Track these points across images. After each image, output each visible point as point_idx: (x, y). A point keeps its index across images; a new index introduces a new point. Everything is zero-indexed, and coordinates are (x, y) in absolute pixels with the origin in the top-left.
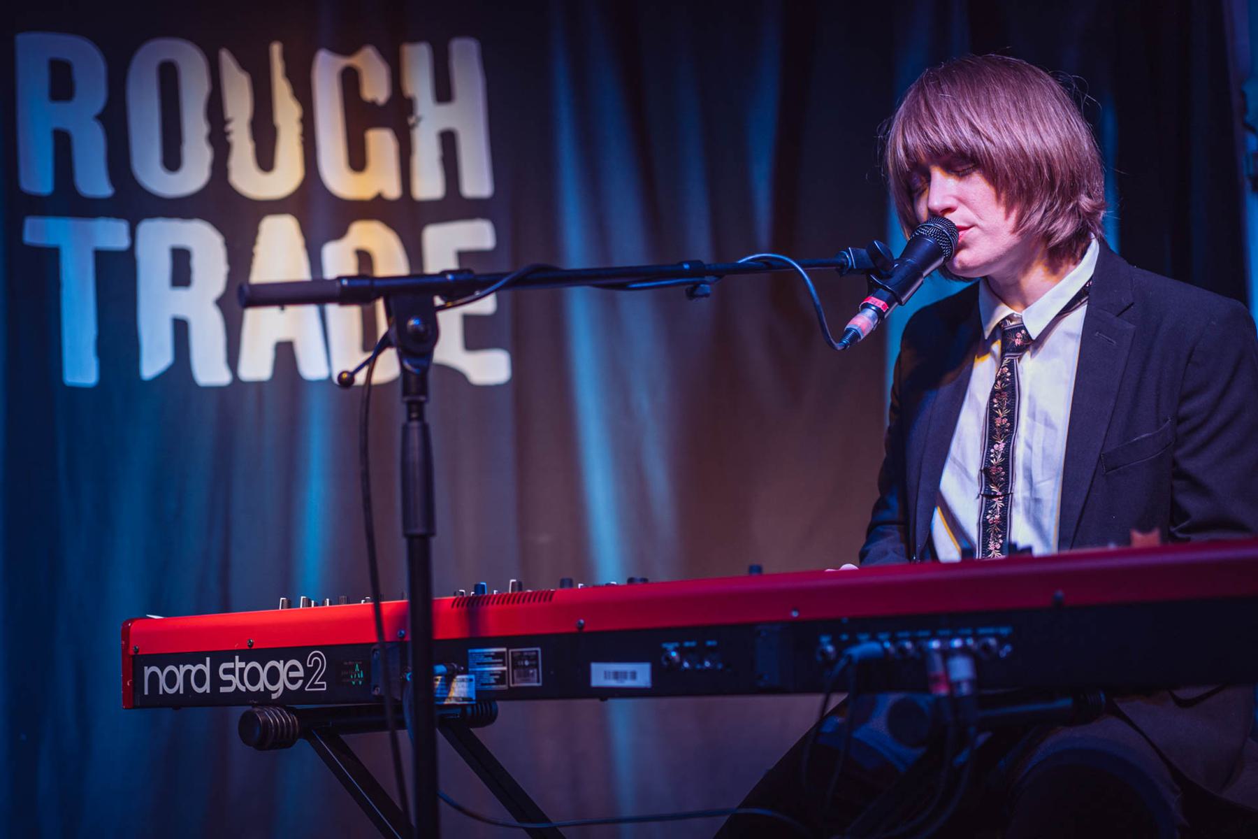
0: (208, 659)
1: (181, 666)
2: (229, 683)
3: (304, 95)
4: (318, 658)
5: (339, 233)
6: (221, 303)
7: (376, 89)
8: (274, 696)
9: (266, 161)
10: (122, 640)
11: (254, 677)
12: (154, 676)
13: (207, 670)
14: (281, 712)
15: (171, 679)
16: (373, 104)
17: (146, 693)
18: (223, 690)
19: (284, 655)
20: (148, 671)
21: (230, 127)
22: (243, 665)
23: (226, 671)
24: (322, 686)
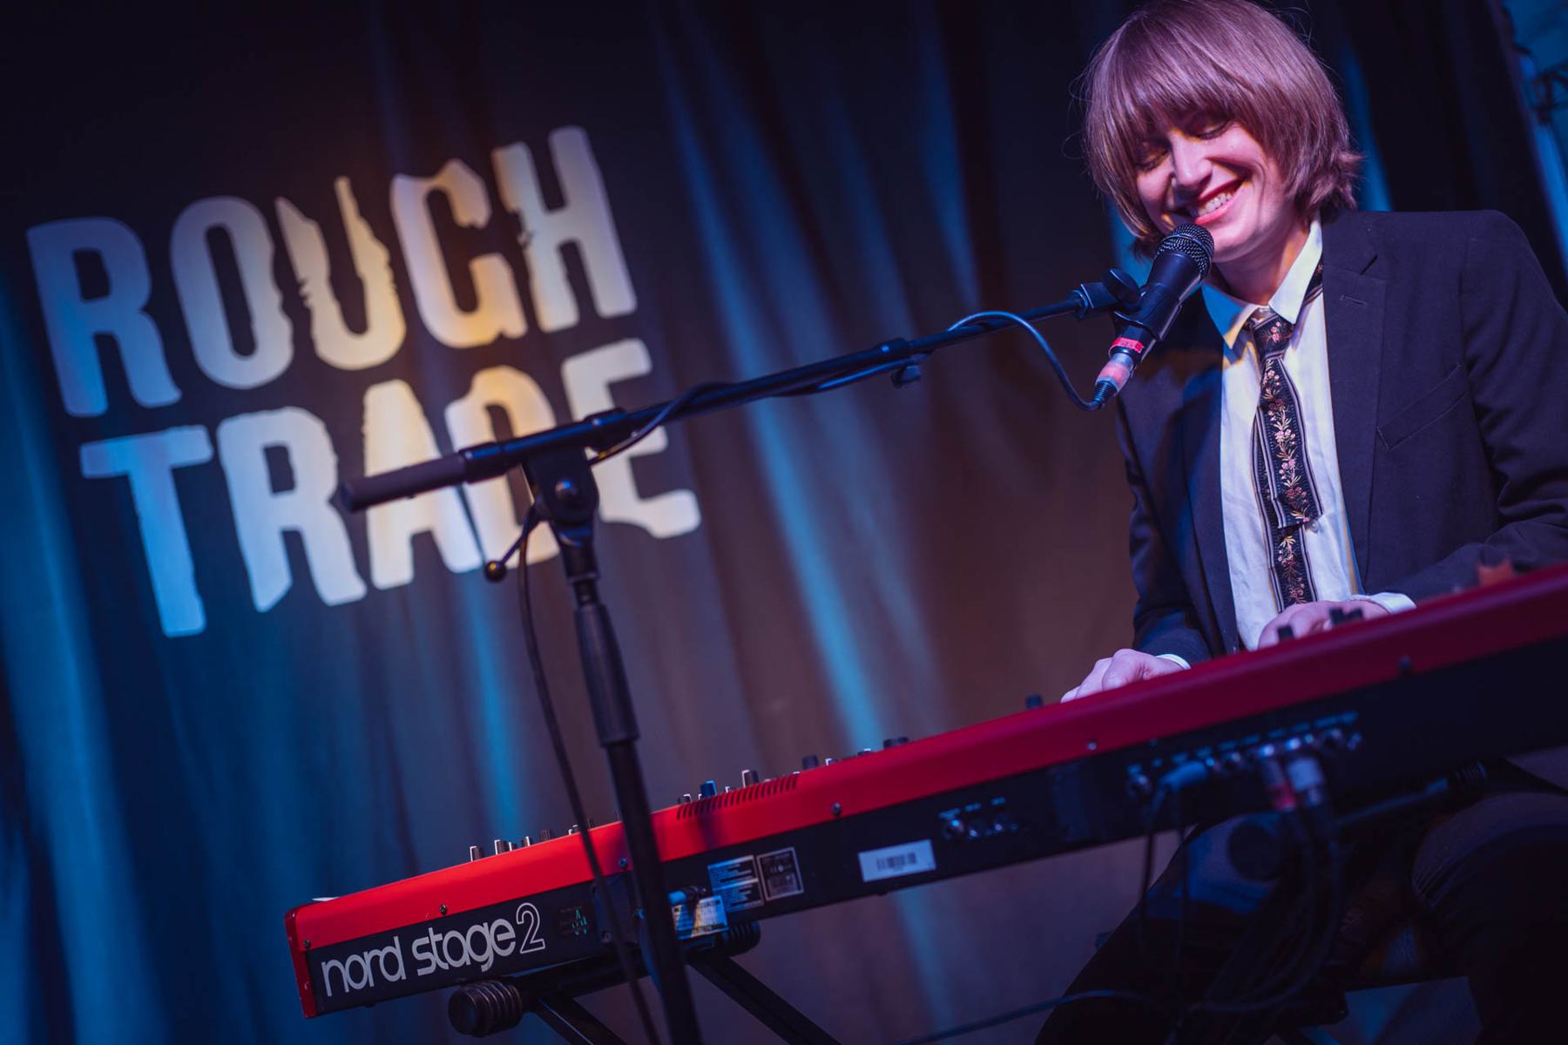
0: (396, 939)
1: (365, 954)
2: (427, 963)
3: (387, 233)
4: (528, 911)
5: (462, 389)
7: (472, 209)
8: (485, 968)
9: (356, 320)
10: (289, 936)
11: (456, 949)
12: (335, 973)
13: (397, 951)
14: (497, 986)
15: (356, 972)
16: (472, 229)
17: (330, 994)
18: (421, 972)
19: (487, 916)
20: (326, 968)
21: (306, 290)
22: (439, 937)
23: (421, 949)
24: (540, 944)
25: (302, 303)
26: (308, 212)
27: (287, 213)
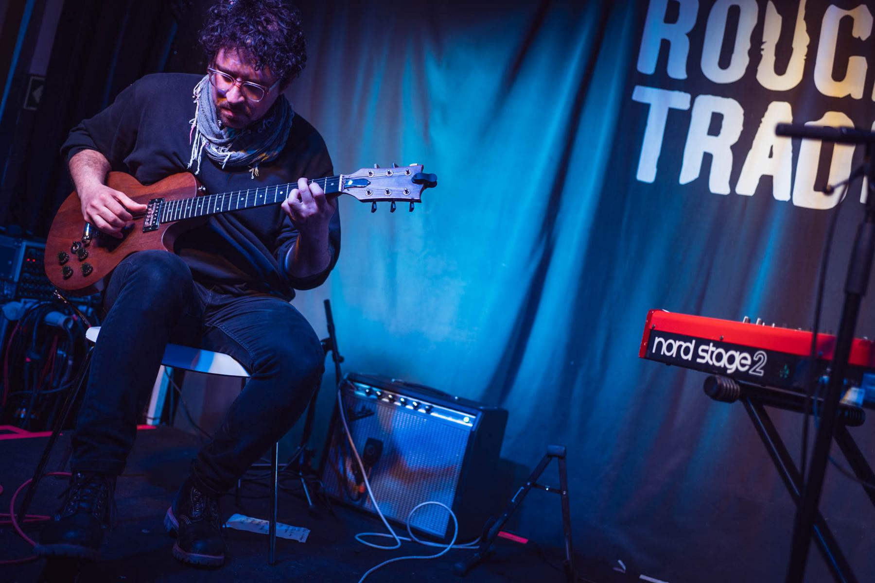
0: (694, 341)
1: (677, 342)
2: (703, 358)
4: (762, 356)
6: (733, 148)
8: (729, 372)
10: (647, 319)
11: (719, 357)
12: (660, 344)
13: (692, 347)
14: (731, 382)
15: (669, 348)
17: (654, 351)
18: (699, 360)
19: (741, 348)
20: (657, 340)
21: (762, 47)
22: (714, 349)
23: (703, 351)
24: (760, 373)
25: (760, 52)
26: (779, 12)
27: (771, 8)
